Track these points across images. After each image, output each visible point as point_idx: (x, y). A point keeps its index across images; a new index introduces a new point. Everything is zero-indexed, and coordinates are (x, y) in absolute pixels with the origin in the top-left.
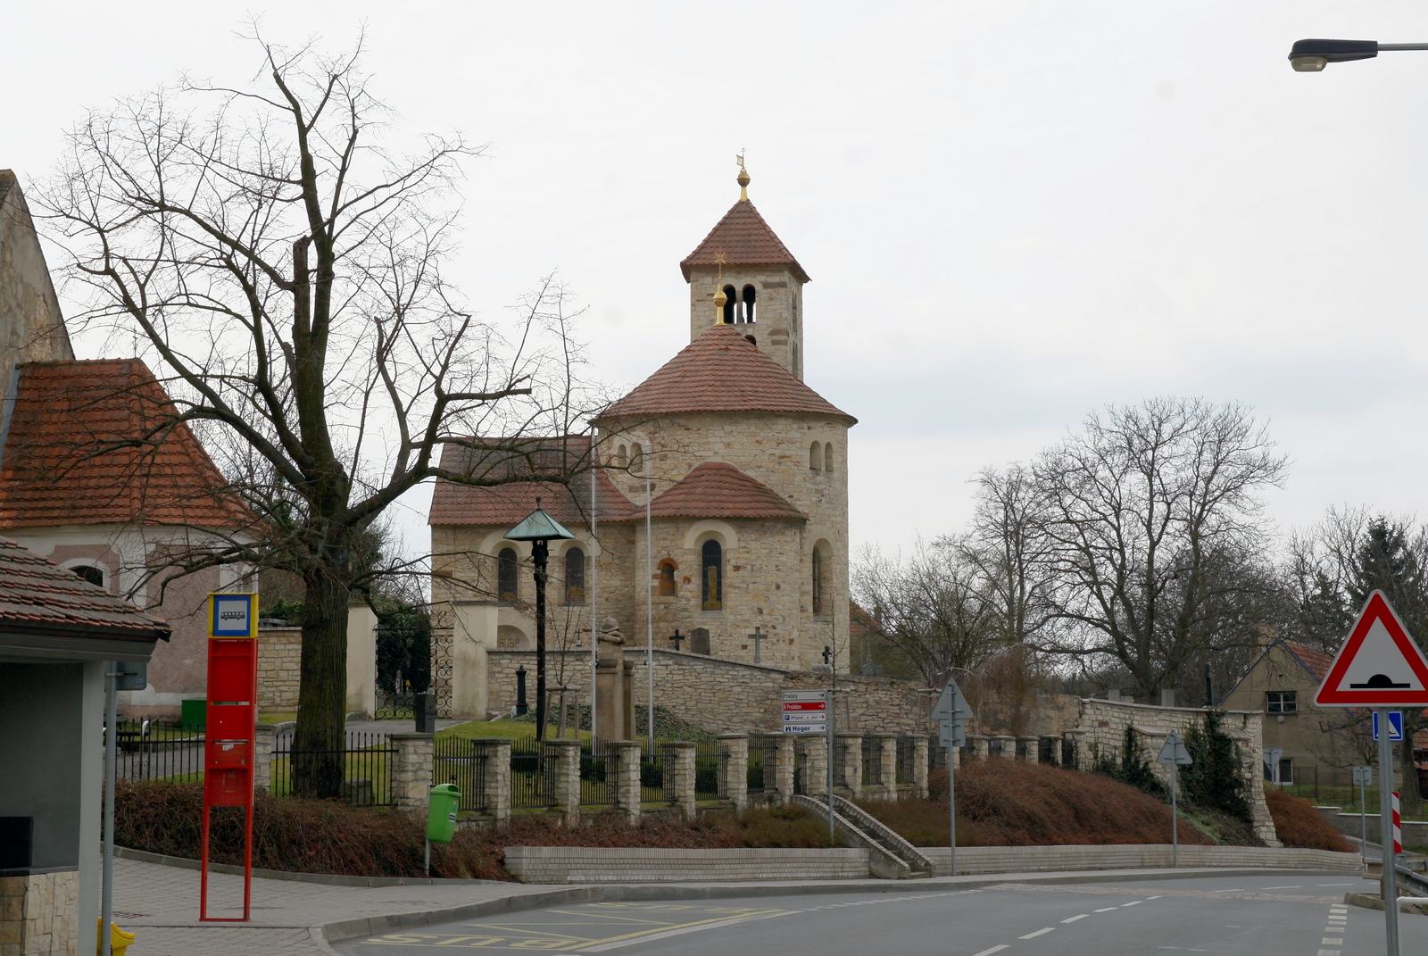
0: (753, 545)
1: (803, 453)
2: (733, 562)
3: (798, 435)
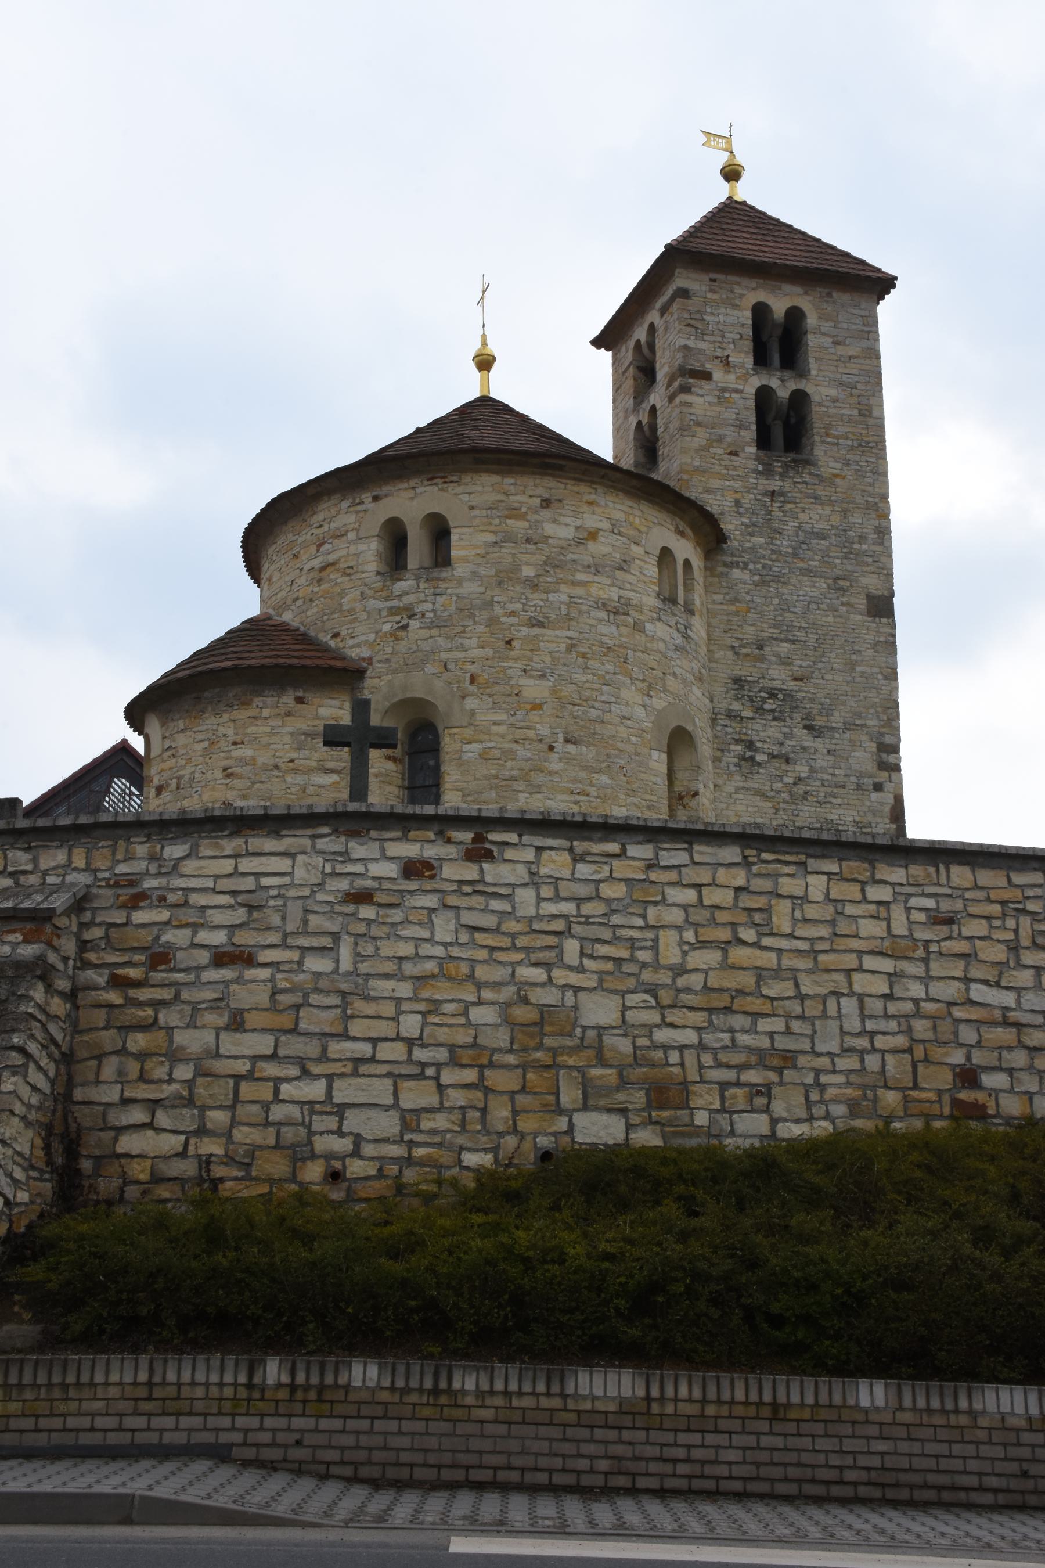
0: (181, 740)
1: (362, 547)
2: (156, 781)
3: (351, 518)
